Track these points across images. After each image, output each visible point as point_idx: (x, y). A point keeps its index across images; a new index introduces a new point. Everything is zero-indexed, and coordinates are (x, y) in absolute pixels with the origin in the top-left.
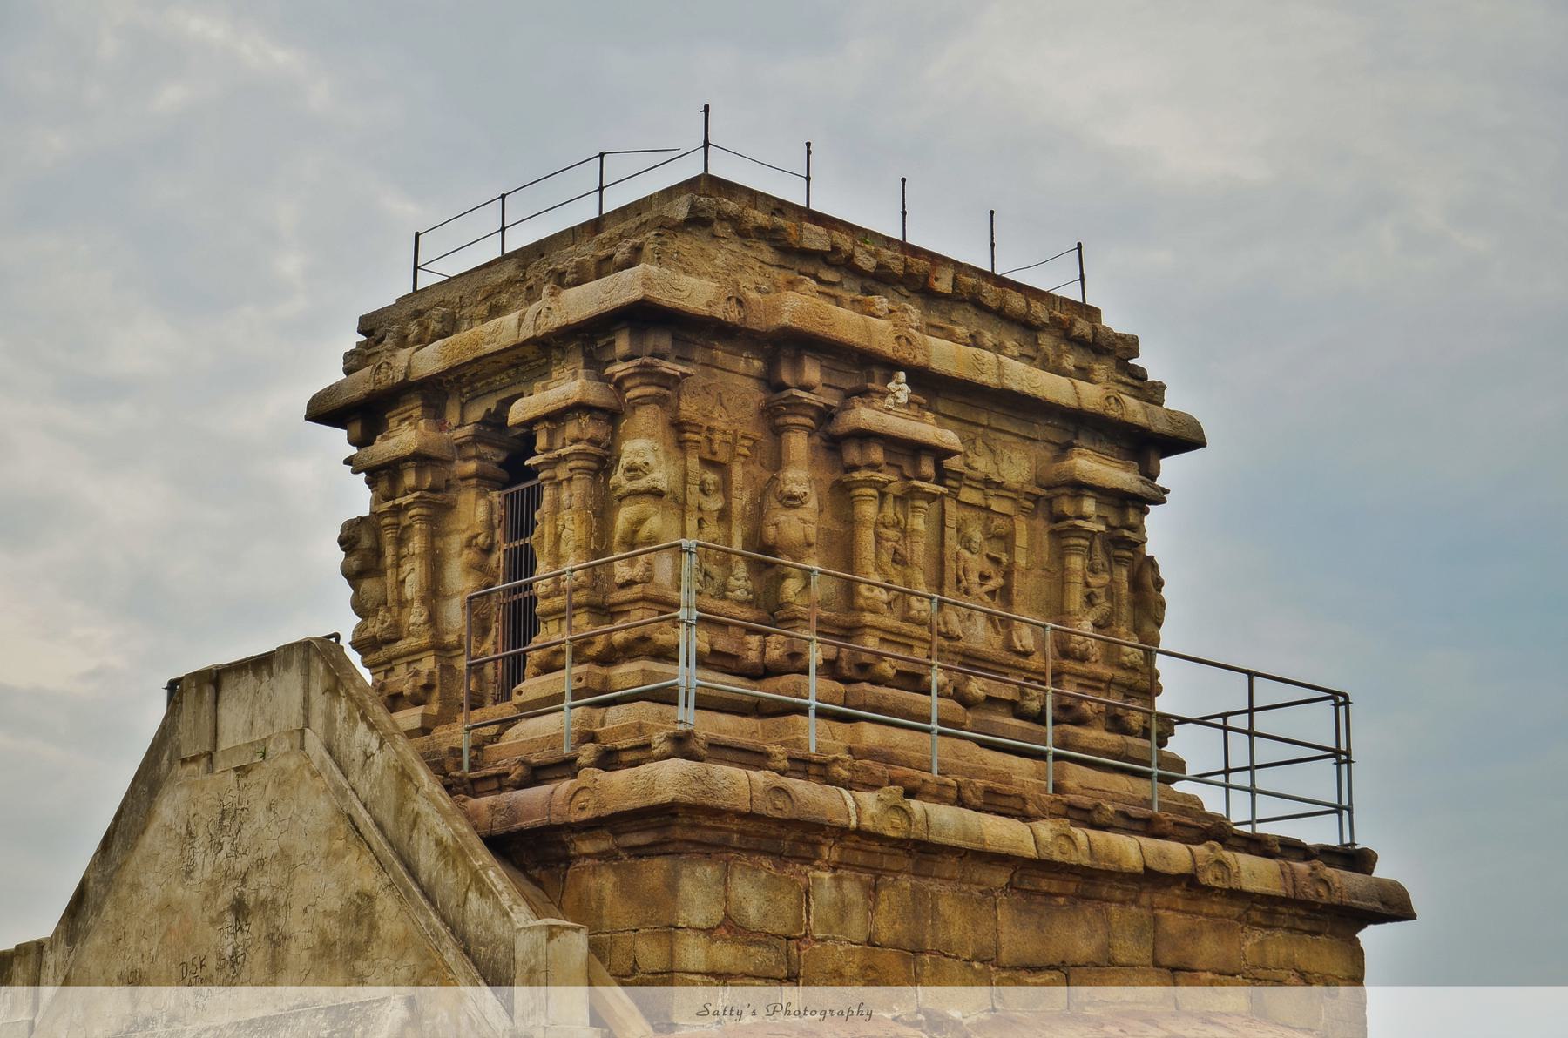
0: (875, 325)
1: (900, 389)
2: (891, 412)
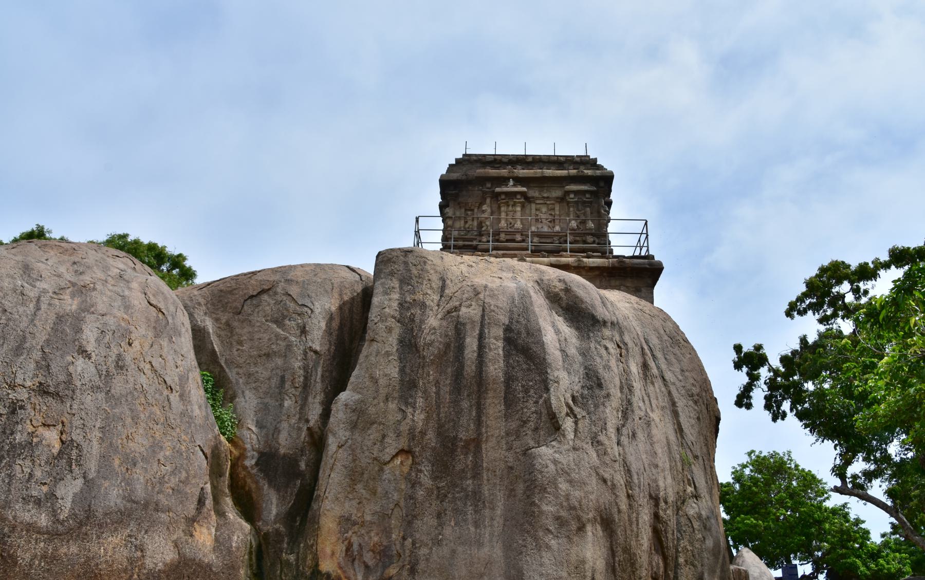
0: (504, 172)
1: (511, 183)
2: (511, 188)
